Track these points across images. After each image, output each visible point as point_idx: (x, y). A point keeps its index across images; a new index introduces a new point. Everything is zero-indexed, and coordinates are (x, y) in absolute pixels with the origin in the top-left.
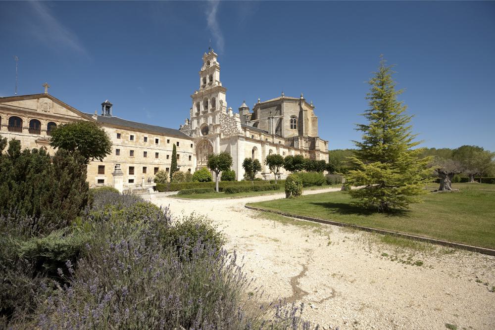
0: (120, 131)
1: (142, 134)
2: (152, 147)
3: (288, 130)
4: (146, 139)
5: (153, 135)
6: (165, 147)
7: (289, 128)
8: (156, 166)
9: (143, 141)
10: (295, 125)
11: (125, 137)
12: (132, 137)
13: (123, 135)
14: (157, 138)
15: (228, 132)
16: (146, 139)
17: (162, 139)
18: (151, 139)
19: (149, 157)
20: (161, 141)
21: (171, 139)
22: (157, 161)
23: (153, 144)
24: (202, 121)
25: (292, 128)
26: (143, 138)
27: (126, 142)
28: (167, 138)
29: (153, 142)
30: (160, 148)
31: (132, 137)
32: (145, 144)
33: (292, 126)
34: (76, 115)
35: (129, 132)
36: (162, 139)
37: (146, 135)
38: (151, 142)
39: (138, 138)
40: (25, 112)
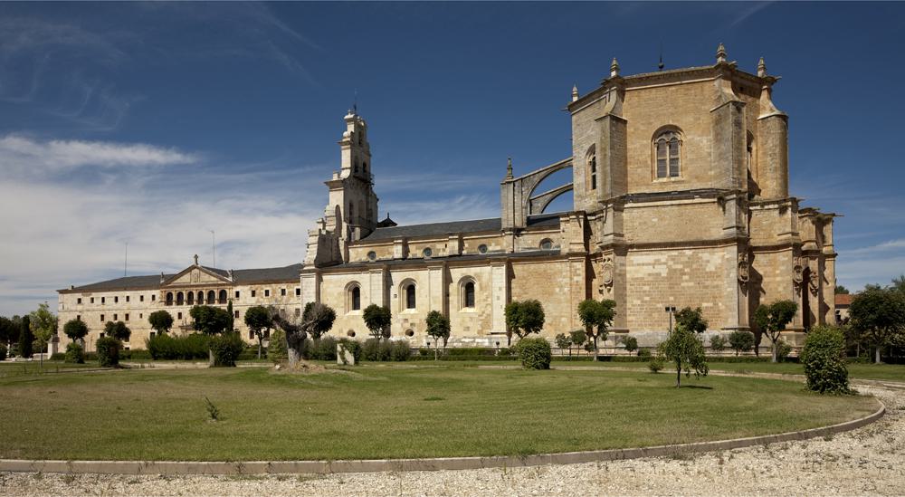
0: (254, 287)
1: (279, 285)
4: (283, 292)
5: (292, 285)
9: (280, 294)
11: (261, 293)
12: (267, 292)
13: (257, 292)
16: (283, 292)
26: (280, 290)
27: (261, 300)
31: (267, 292)
34: (215, 279)
35: (263, 286)
38: (291, 294)
39: (274, 292)
40: (184, 287)
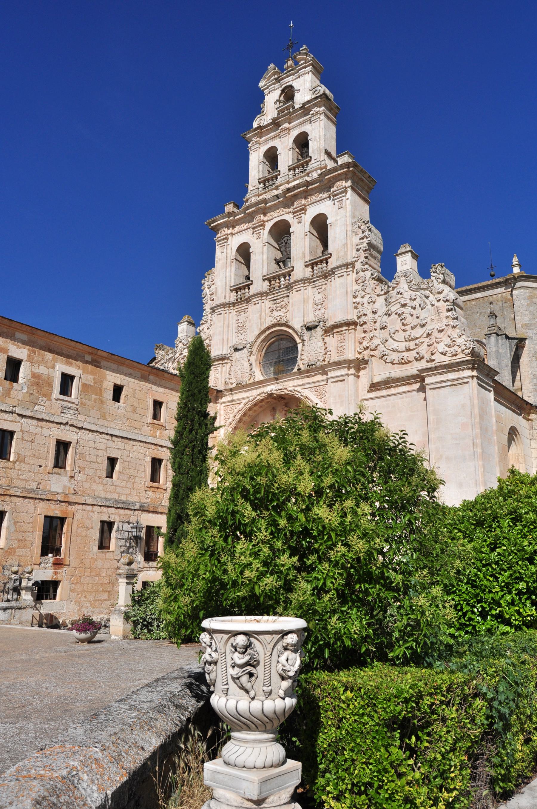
2: (40, 411)
5: (49, 356)
6: (104, 417)
8: (56, 511)
14: (70, 370)
15: (408, 350)
17: (89, 379)
18: (42, 370)
19: (20, 459)
20: (85, 387)
21: (131, 385)
22: (58, 484)
23: (48, 396)
24: (259, 317)
28: (112, 378)
29: (50, 385)
30: (81, 420)
32: (7, 393)
36: (89, 379)
37: (18, 351)
38: (39, 383)
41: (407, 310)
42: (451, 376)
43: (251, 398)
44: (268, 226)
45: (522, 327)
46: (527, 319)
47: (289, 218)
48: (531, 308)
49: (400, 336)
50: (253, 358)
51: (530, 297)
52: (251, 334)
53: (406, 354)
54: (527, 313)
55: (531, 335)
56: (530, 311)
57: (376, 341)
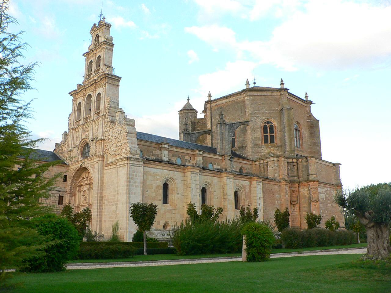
3: (259, 146)
7: (260, 142)
10: (272, 138)
25: (266, 142)
33: (266, 138)
41: (117, 135)
42: (123, 163)
43: (76, 168)
44: (87, 95)
45: (248, 115)
46: (251, 111)
47: (91, 93)
48: (253, 106)
49: (115, 145)
50: (79, 151)
51: (253, 100)
52: (77, 142)
53: (115, 153)
54: (251, 108)
55: (252, 119)
56: (252, 107)
57: (109, 147)
